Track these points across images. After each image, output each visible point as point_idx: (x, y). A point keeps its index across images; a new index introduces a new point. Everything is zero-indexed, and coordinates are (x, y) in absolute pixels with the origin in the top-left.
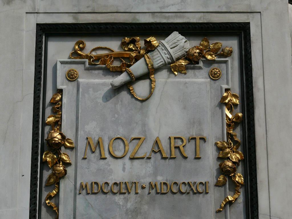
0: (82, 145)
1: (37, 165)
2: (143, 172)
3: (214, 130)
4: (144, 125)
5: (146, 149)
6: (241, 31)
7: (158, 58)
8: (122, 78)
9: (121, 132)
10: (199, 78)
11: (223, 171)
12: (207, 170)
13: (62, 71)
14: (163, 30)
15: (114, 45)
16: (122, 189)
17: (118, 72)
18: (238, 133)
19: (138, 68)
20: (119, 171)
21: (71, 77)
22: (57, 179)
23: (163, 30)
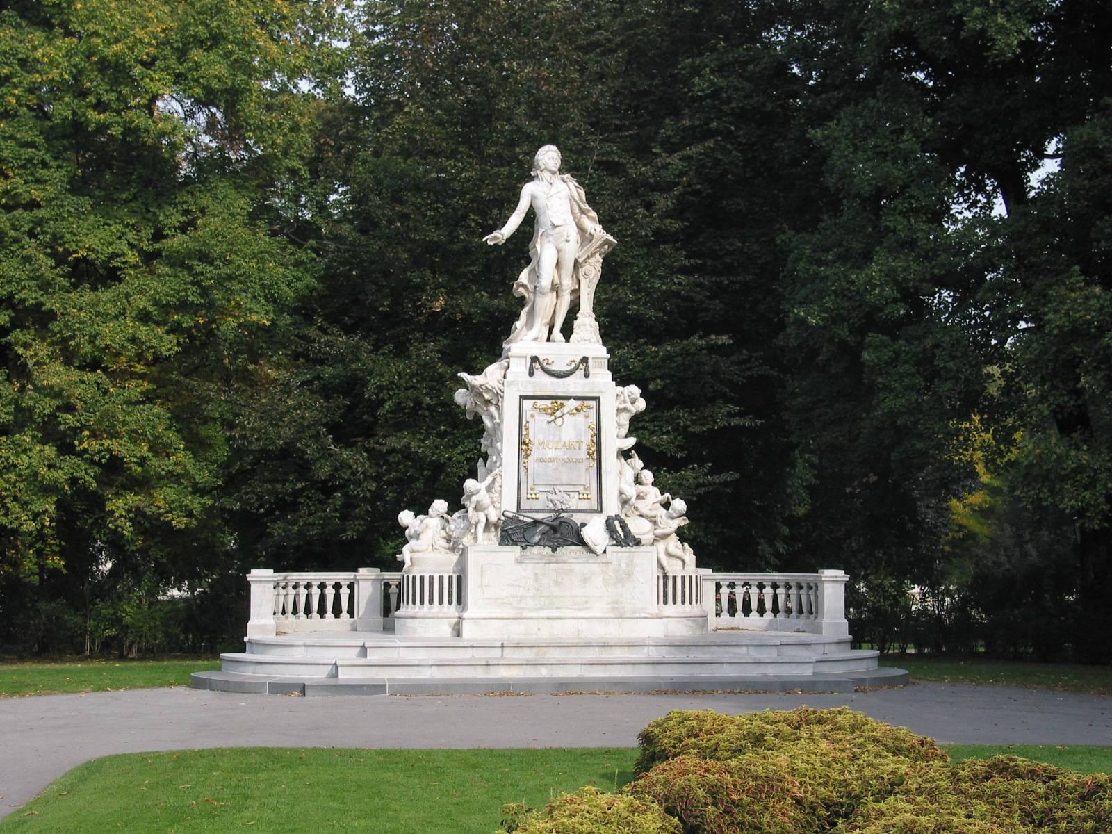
0: (536, 443)
1: (520, 450)
2: (559, 454)
3: (586, 437)
4: (560, 436)
5: (560, 446)
6: (597, 399)
7: (566, 410)
8: (553, 418)
9: (551, 438)
10: (580, 418)
11: (589, 454)
12: (583, 454)
13: (529, 413)
14: (568, 398)
15: (548, 403)
16: (552, 460)
17: (551, 415)
18: (595, 439)
19: (558, 414)
20: (550, 453)
21: (532, 416)
22: (527, 456)
23: (568, 398)
